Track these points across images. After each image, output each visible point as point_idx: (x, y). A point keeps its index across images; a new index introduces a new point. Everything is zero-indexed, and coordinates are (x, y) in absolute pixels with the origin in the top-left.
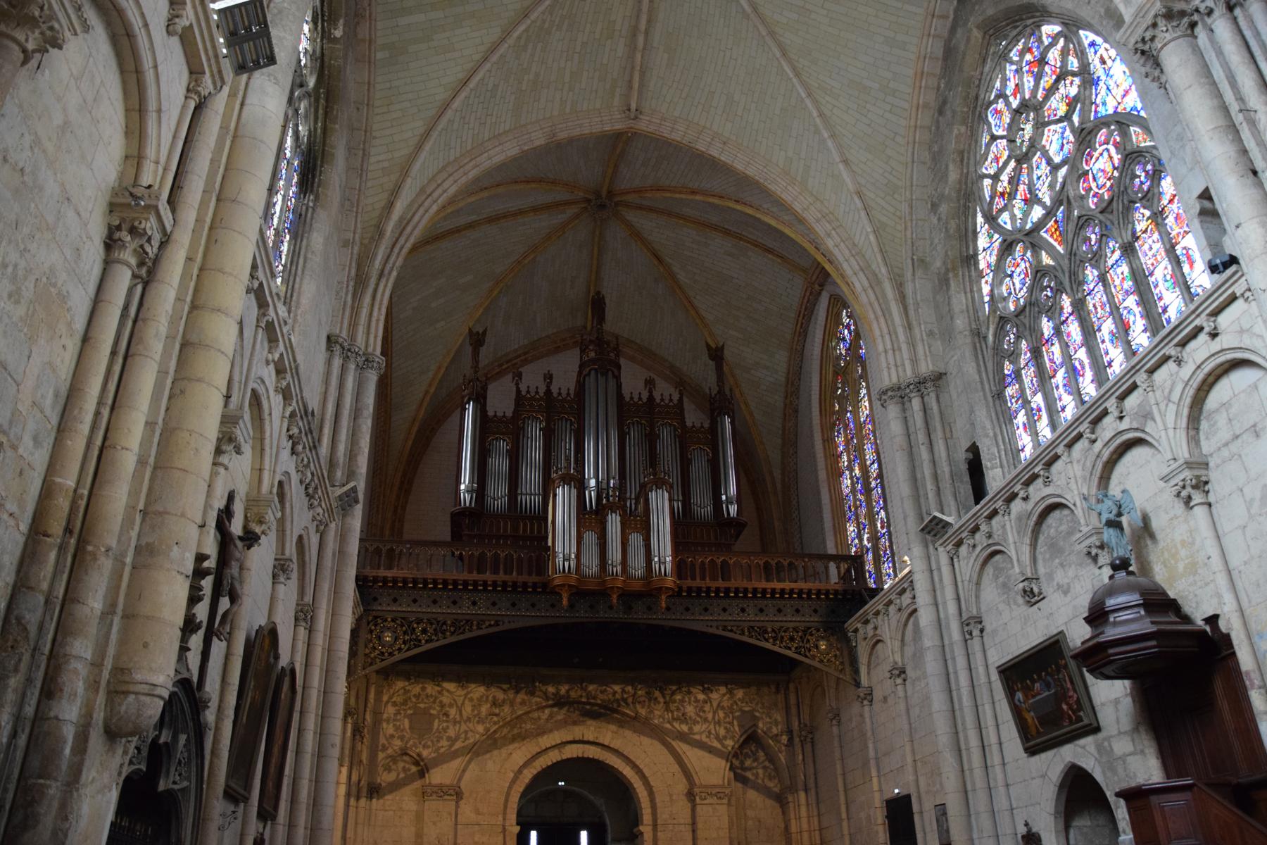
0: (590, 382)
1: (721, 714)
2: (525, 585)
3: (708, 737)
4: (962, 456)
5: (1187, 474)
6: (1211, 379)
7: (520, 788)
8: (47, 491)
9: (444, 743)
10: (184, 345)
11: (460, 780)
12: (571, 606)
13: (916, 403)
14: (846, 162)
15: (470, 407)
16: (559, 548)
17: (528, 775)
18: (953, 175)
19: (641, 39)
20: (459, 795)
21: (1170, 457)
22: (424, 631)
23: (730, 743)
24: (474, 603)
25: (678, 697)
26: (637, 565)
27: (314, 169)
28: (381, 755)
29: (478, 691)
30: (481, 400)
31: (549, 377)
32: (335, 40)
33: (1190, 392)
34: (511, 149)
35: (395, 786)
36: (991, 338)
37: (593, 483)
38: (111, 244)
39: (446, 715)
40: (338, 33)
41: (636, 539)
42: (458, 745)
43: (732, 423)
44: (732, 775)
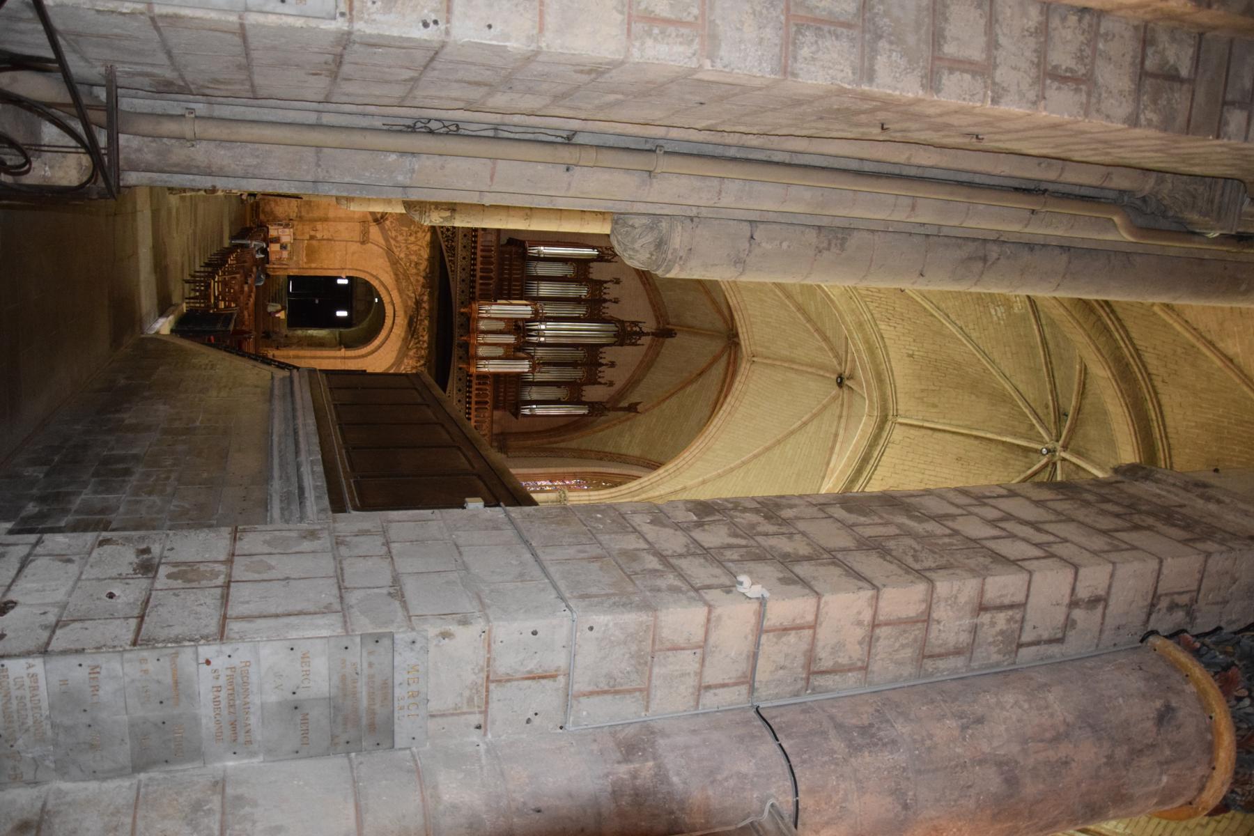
0: (612, 327)
2: (474, 287)
7: (368, 278)
9: (394, 234)
12: (462, 314)
14: (704, 482)
15: (596, 252)
16: (494, 307)
20: (363, 243)
26: (482, 351)
30: (600, 259)
37: (543, 327)
41: (500, 351)
42: (393, 242)
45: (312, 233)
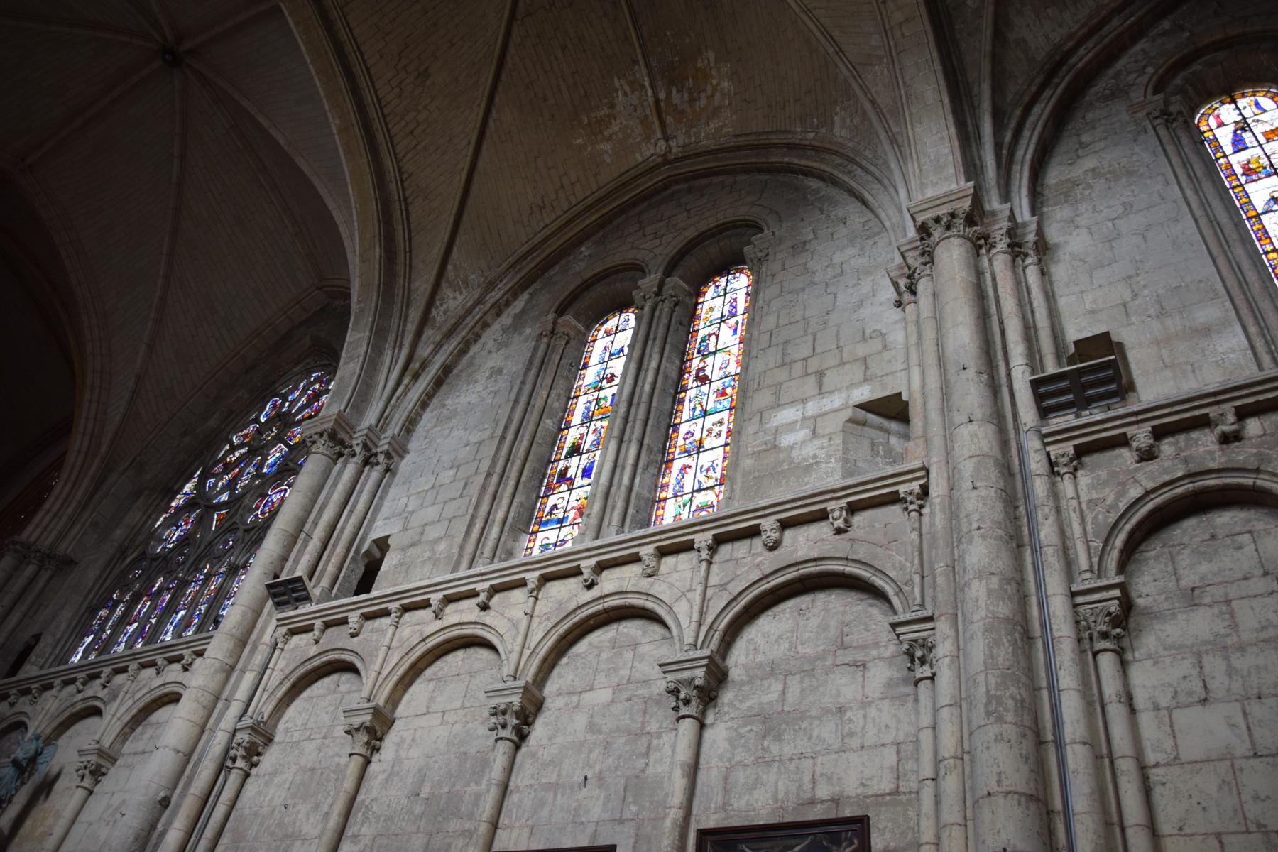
4: (26, 636)
5: (94, 759)
6: (166, 699)
13: (30, 570)
18: (212, 423)
21: (97, 738)
33: (147, 699)
36: (128, 560)
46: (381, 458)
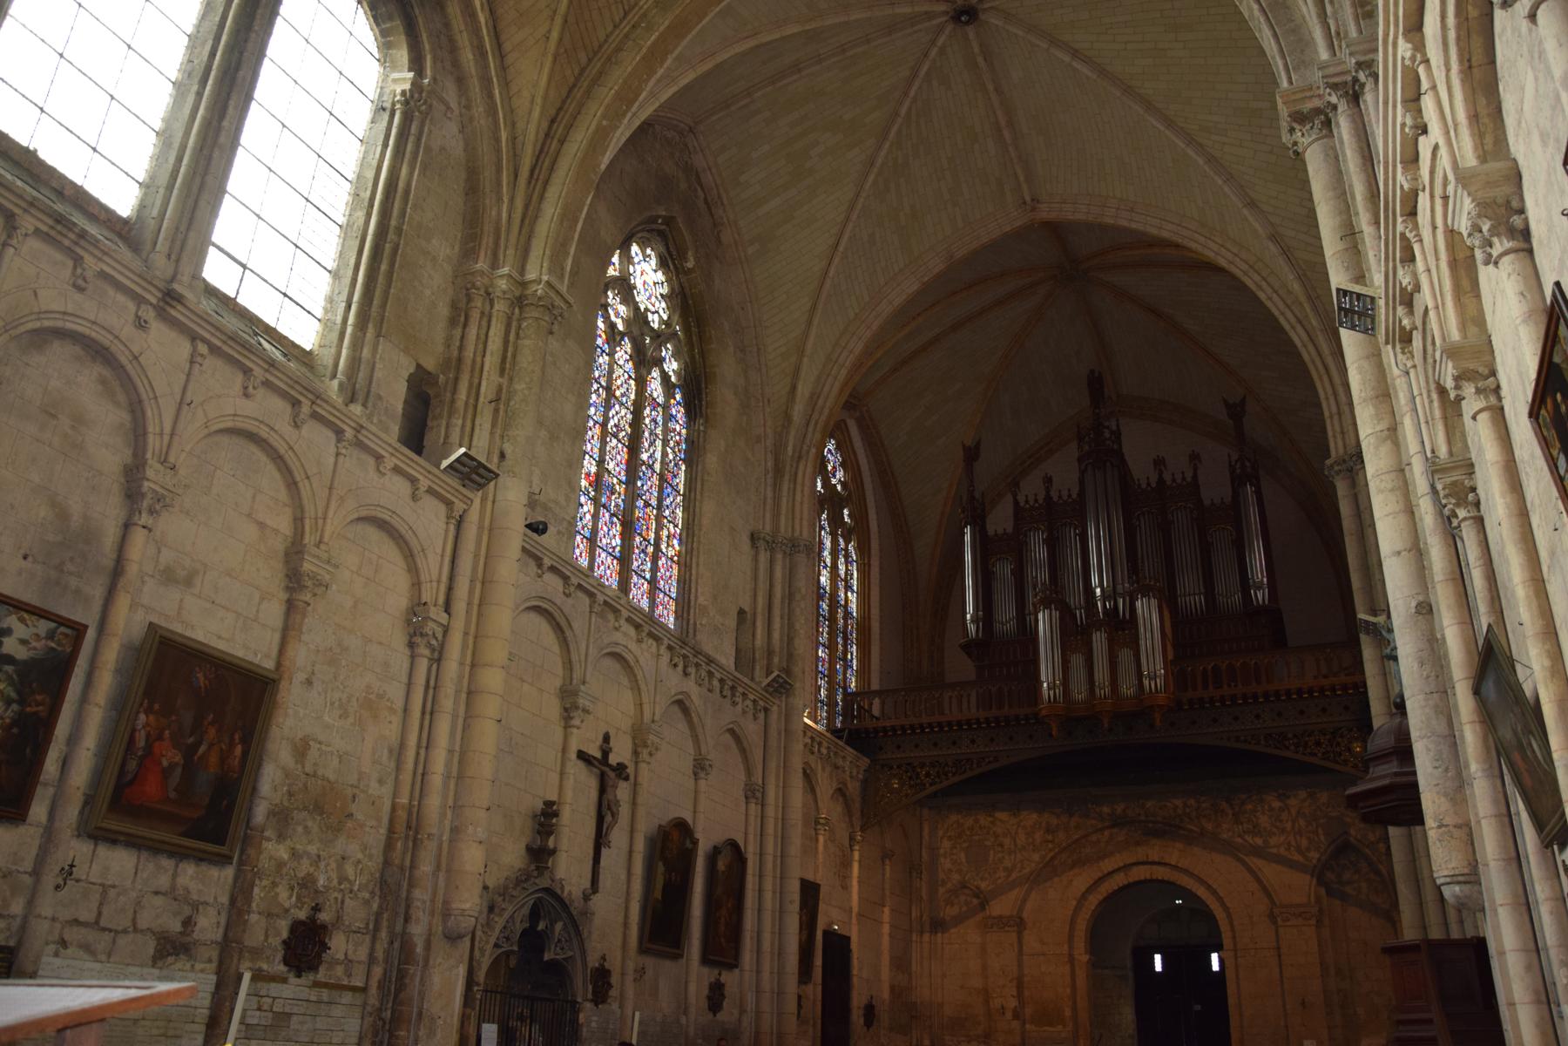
1: (1302, 822)
3: (1288, 849)
8: (394, 808)
10: (469, 693)
11: (1021, 909)
14: (1252, 204)
15: (968, 530)
17: (1094, 901)
19: (1007, 134)
22: (928, 775)
23: (1314, 855)
24: (973, 742)
25: (1249, 807)
27: (700, 394)
28: (941, 890)
29: (1030, 818)
31: (1048, 480)
32: (690, 271)
34: (910, 286)
35: (959, 920)
38: (411, 645)
39: (1001, 845)
40: (690, 264)
41: (1125, 655)
42: (1014, 875)
43: (1258, 493)
44: (1323, 891)
45: (1009, 1015)
46: (1362, 76)
